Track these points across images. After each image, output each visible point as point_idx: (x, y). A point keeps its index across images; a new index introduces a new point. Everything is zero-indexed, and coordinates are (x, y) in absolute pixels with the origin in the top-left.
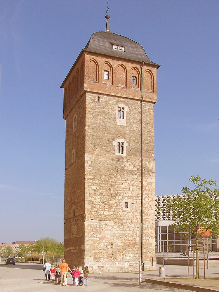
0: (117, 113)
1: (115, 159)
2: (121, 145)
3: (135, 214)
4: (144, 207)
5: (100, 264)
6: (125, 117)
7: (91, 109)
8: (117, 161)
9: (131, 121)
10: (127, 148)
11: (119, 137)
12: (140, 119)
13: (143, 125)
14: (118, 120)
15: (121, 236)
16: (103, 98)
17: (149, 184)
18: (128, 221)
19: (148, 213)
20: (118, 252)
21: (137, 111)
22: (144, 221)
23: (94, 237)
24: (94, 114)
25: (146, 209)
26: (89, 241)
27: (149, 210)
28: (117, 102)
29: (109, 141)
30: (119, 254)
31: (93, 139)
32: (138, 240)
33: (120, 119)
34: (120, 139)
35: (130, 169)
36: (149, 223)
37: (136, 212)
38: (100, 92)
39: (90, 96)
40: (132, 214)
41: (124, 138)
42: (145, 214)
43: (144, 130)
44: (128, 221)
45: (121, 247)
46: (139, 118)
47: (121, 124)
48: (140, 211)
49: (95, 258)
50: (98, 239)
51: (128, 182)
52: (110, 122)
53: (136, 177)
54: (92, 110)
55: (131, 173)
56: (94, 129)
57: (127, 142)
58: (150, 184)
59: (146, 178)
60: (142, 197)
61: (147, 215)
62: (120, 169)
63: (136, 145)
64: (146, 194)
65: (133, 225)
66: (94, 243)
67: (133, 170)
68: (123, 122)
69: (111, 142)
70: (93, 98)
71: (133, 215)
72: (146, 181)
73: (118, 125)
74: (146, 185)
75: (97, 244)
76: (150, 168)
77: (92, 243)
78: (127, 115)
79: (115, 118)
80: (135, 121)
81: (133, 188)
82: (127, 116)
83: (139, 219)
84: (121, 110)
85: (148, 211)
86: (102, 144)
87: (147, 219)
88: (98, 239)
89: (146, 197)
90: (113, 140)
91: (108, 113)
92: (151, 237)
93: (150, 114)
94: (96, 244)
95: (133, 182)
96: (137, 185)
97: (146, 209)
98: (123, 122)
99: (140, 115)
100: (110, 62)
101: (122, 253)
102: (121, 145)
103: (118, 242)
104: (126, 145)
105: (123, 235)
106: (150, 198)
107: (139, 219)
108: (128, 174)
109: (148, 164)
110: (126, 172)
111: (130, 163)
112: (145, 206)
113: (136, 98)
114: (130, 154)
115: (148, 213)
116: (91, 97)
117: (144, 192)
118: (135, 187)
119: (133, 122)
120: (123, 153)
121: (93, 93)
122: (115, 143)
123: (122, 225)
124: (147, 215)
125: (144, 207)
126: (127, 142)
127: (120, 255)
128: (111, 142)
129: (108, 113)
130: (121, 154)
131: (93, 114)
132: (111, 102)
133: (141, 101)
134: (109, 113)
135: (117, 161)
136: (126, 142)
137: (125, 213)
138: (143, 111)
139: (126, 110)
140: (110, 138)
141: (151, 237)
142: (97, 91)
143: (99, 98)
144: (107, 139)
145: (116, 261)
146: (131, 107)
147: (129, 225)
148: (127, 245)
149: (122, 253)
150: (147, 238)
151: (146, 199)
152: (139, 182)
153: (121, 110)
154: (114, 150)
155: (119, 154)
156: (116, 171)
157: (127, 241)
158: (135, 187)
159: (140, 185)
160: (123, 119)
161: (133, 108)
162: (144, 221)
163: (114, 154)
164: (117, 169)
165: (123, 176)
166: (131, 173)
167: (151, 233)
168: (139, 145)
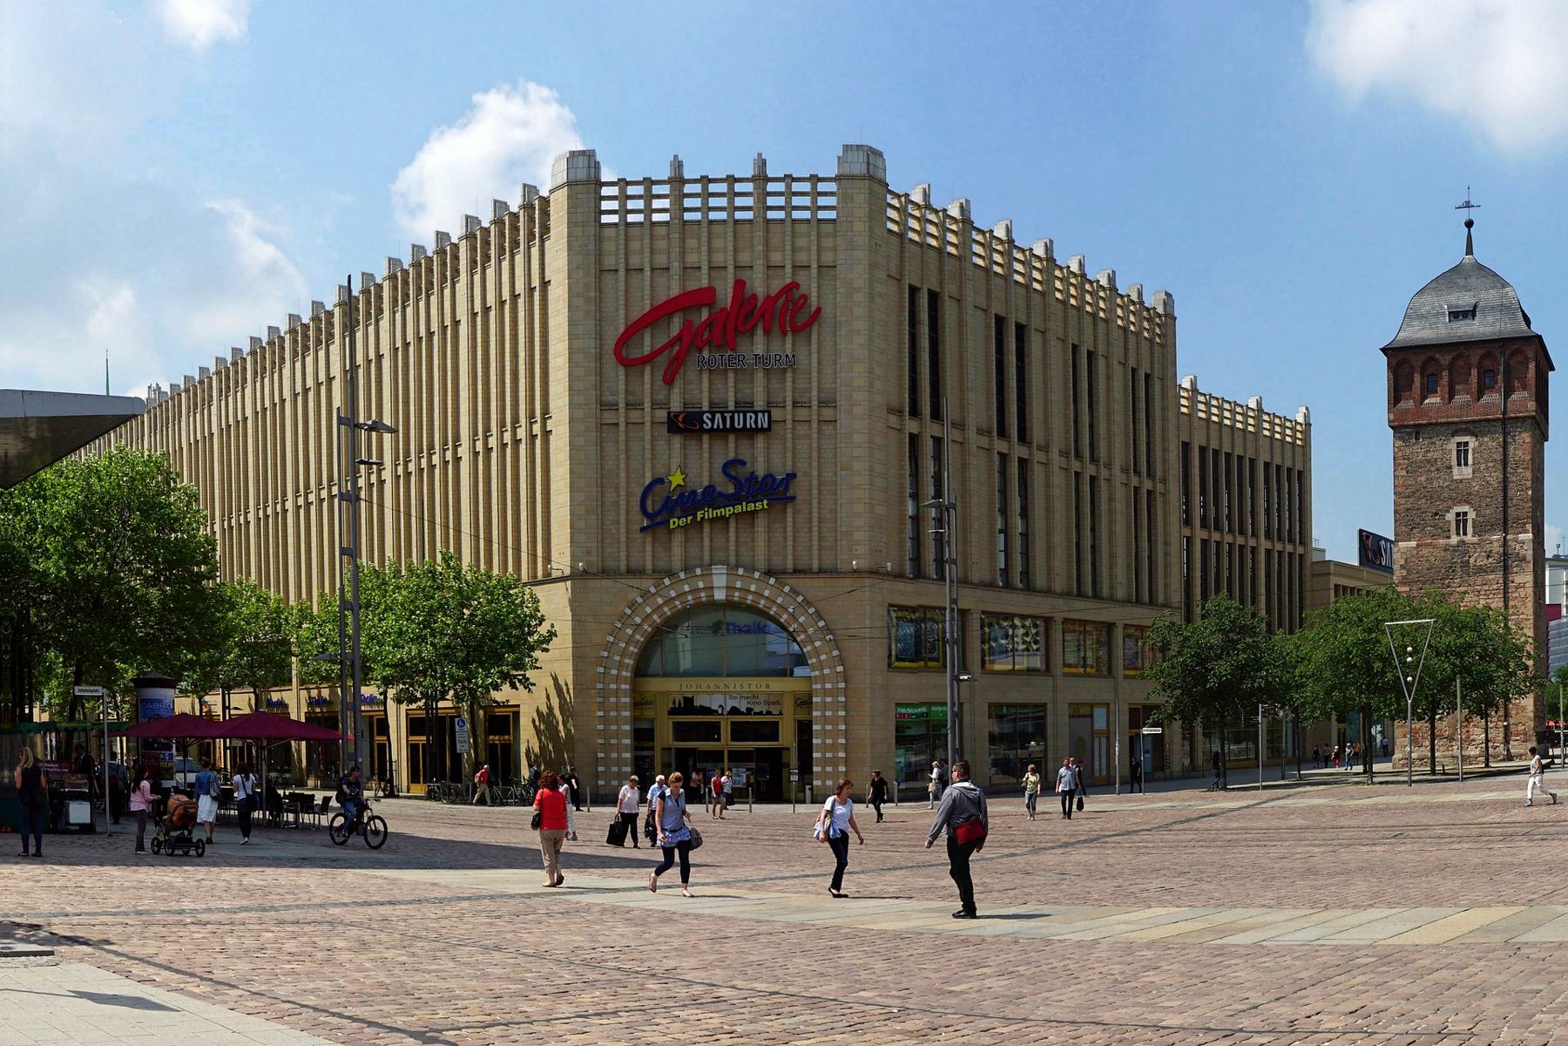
0: (1454, 453)
2: (1461, 519)
6: (1470, 461)
11: (1460, 503)
14: (1455, 470)
46: (1499, 457)
55: (1482, 570)
68: (1463, 473)
76: (1522, 552)
79: (1450, 467)
84: (1462, 450)
102: (1461, 519)
104: (1472, 515)
122: (1450, 516)
139: (1471, 446)
153: (1462, 450)
166: (1482, 570)
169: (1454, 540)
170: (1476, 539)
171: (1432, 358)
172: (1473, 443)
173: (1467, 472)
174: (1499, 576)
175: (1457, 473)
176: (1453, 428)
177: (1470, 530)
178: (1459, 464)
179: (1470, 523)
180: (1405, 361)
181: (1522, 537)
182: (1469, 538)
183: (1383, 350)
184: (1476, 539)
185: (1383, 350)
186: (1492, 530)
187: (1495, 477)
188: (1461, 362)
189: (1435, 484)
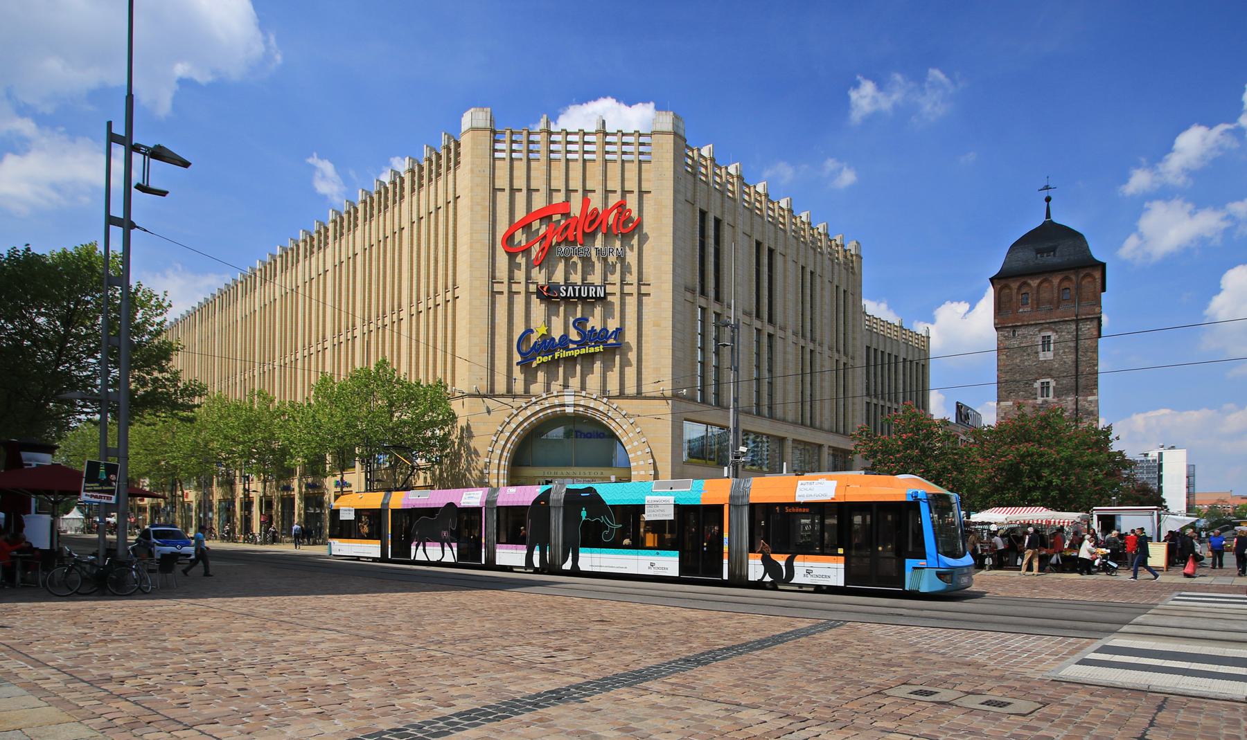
2: (1045, 387)
14: (1041, 355)
16: (1019, 332)
29: (1029, 384)
46: (1072, 344)
84: (1046, 342)
98: (1049, 355)
102: (1045, 387)
104: (1053, 384)
122: (1037, 385)
133: (1077, 321)
139: (1053, 338)
169: (1040, 400)
171: (1025, 283)
172: (1054, 337)
173: (1049, 355)
175: (1042, 356)
177: (1051, 394)
186: (1067, 394)
187: (1070, 358)
188: (1045, 285)
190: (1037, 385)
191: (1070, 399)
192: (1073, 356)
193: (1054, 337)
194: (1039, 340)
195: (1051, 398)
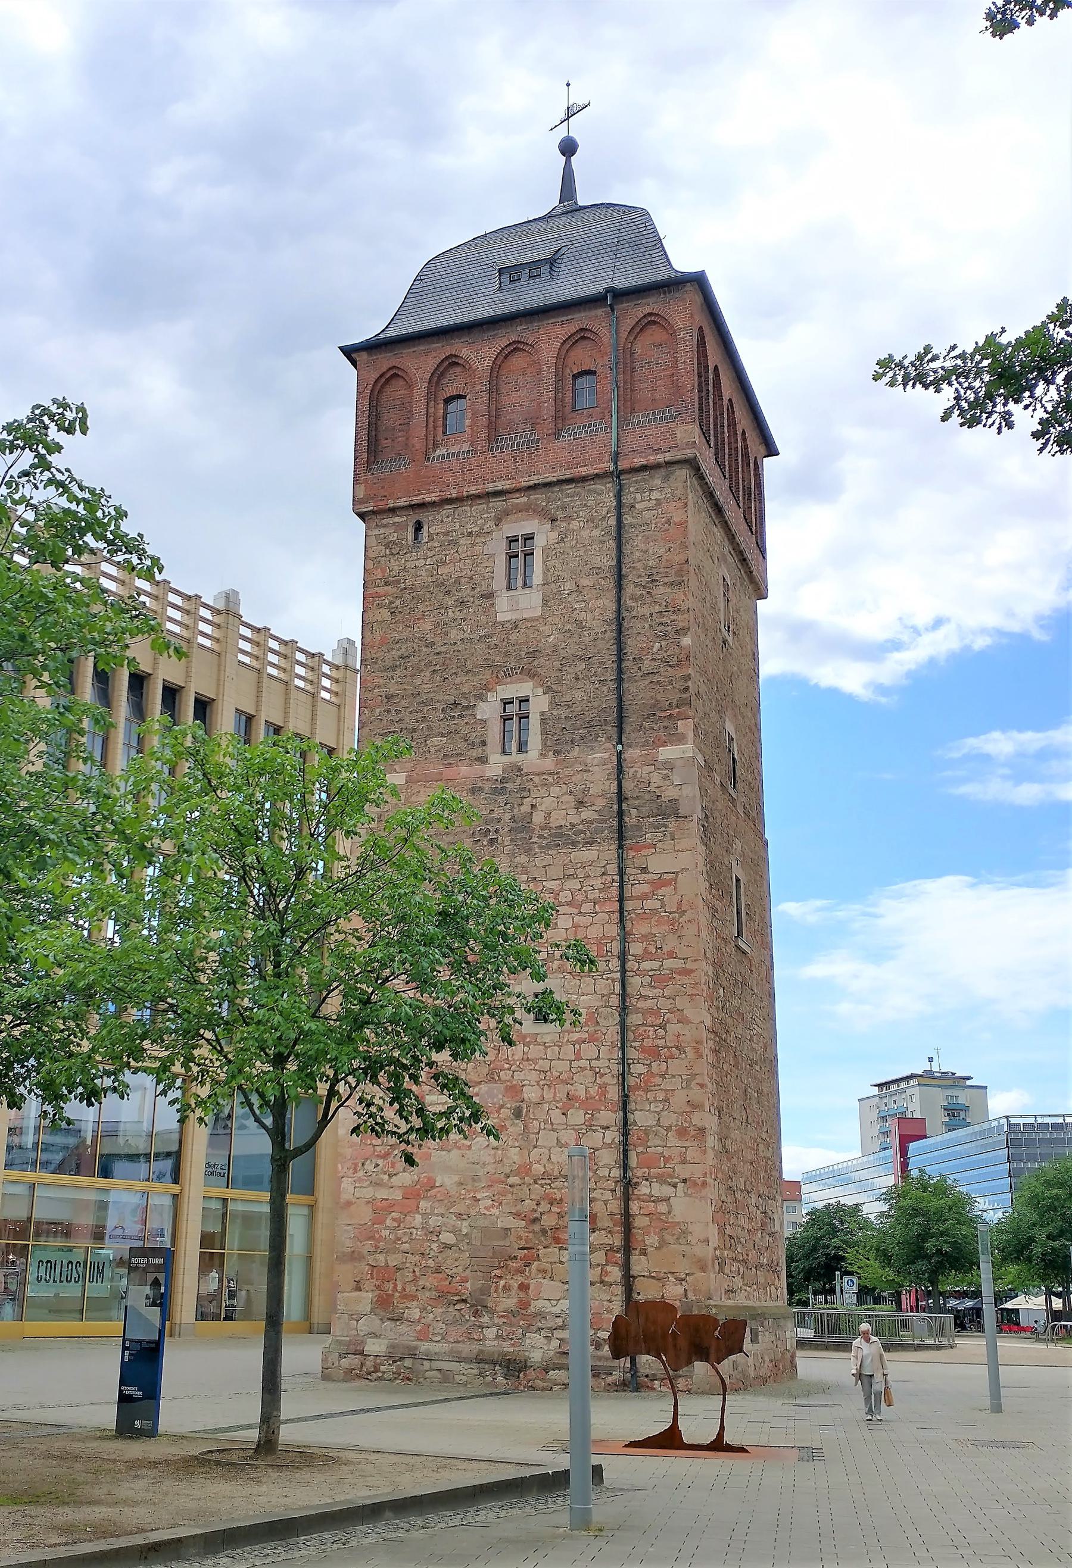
0: (501, 561)
1: (487, 787)
3: (589, 1051)
4: (638, 1011)
5: (404, 1334)
6: (537, 578)
7: (386, 584)
8: (495, 791)
9: (568, 586)
10: (543, 721)
12: (614, 563)
13: (629, 590)
15: (513, 1180)
16: (435, 524)
17: (660, 883)
18: (548, 1095)
19: (661, 1042)
20: (497, 1272)
21: (596, 533)
22: (638, 1088)
23: (378, 1184)
24: (398, 602)
25: (650, 1020)
26: (353, 1208)
27: (663, 1027)
28: (498, 521)
30: (502, 1283)
31: (389, 711)
32: (606, 1203)
33: (511, 593)
34: (511, 683)
35: (558, 819)
36: (667, 1100)
37: (592, 1039)
38: (415, 500)
39: (382, 531)
40: (569, 1051)
41: (532, 674)
42: (644, 1050)
43: (638, 608)
44: (548, 1095)
45: (512, 1238)
46: (606, 560)
47: (515, 616)
48: (612, 1033)
49: (383, 1303)
50: (398, 1195)
51: (549, 885)
52: (465, 620)
53: (588, 854)
54: (386, 588)
55: (562, 838)
56: (394, 668)
57: (545, 693)
58: (667, 883)
59: (644, 852)
60: (623, 957)
61: (654, 1053)
62: (506, 829)
63: (592, 695)
64: (645, 938)
65: (577, 1117)
66: (379, 1219)
67: (575, 819)
69: (468, 707)
70: (394, 537)
71: (578, 1057)
72: (644, 870)
73: (503, 624)
74: (646, 888)
75: (394, 1220)
76: (670, 793)
77: (365, 1215)
78: (544, 562)
79: (489, 596)
80: (585, 582)
81: (576, 911)
82: (546, 569)
83: (607, 1079)
85: (661, 1032)
86: (429, 728)
87: (658, 1080)
88: (398, 1195)
89: (646, 956)
90: (481, 697)
91: (457, 581)
92: (684, 1181)
93: (669, 522)
94: (388, 1222)
95: (574, 884)
96: (596, 894)
97: (650, 1020)
99: (612, 544)
100: (465, 352)
101: (520, 1279)
103: (494, 1211)
104: (539, 704)
105: (524, 1170)
106: (672, 955)
107: (607, 1079)
108: (548, 847)
109: (656, 779)
110: (541, 837)
111: (555, 790)
112: (641, 1004)
113: (583, 471)
114: (557, 742)
115: (661, 1042)
116: (388, 531)
117: (639, 929)
118: (587, 907)
119: (578, 589)
120: (522, 748)
121: (393, 510)
122: (488, 710)
123: (518, 1114)
124: (654, 1053)
125: (638, 1011)
126: (548, 690)
127: (507, 1288)
128: (468, 707)
129: (457, 581)
130: (515, 758)
131: (391, 603)
132: (470, 528)
134: (463, 580)
135: (495, 791)
136: (540, 691)
137: (534, 1051)
138: (628, 519)
139: (540, 541)
140: (465, 689)
141: (684, 1181)
142: (403, 502)
143: (418, 527)
144: (452, 699)
145: (485, 1319)
146: (568, 518)
147: (556, 1116)
148: (544, 1232)
149: (520, 1279)
150: (657, 1190)
151: (646, 965)
152: (609, 879)
153: (519, 550)
154: (484, 743)
155: (506, 759)
156: (492, 841)
157: (544, 1207)
158: (587, 907)
159: (614, 892)
160: (527, 591)
161: (575, 525)
162: (638, 1088)
163: (482, 760)
164: (497, 831)
165: (522, 859)
167: (684, 1162)
168: (609, 690)
169: (496, 765)
170: (549, 763)
171: (452, 362)
172: (544, 536)
174: (610, 851)
176: (498, 504)
177: (535, 740)
178: (509, 587)
179: (534, 723)
180: (393, 375)
181: (666, 753)
182: (533, 758)
183: (350, 352)
184: (549, 763)
185: (350, 352)
188: (518, 361)
189: (454, 635)
190: (488, 710)
191: (599, 757)
192: (608, 603)
193: (544, 536)
194: (497, 547)
195: (533, 758)
